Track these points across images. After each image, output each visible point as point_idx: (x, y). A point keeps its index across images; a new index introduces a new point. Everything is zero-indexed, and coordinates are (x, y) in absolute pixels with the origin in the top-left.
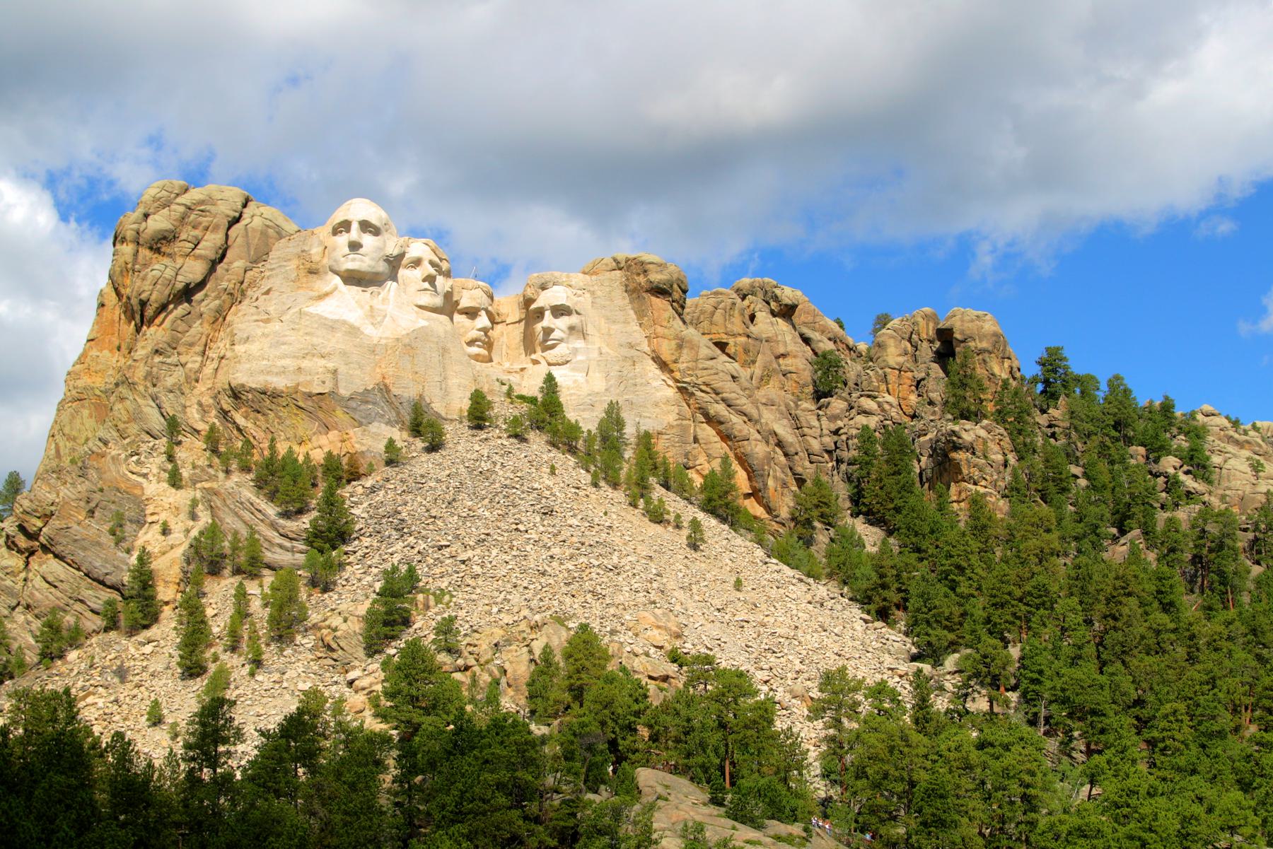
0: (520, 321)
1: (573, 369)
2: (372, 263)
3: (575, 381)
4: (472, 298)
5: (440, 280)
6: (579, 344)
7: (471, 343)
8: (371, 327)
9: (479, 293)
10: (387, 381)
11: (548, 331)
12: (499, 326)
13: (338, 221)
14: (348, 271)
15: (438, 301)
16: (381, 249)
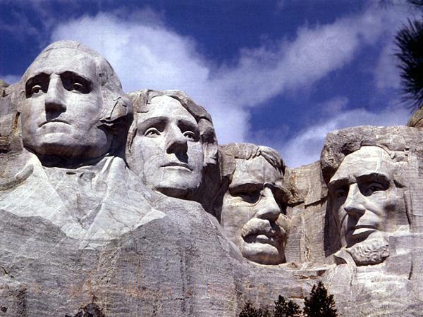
0: (321, 201)
1: (390, 270)
2: (81, 133)
3: (389, 288)
4: (250, 171)
5: (194, 148)
6: (402, 231)
7: (251, 237)
8: (76, 225)
9: (258, 162)
10: (99, 303)
11: (355, 214)
12: (296, 209)
13: (32, 76)
14: (45, 145)
15: (192, 180)
16: (91, 111)
